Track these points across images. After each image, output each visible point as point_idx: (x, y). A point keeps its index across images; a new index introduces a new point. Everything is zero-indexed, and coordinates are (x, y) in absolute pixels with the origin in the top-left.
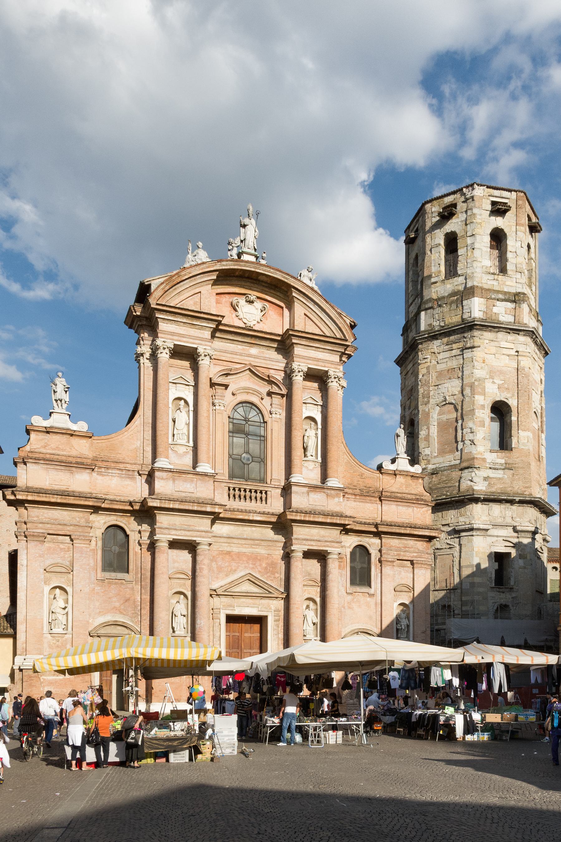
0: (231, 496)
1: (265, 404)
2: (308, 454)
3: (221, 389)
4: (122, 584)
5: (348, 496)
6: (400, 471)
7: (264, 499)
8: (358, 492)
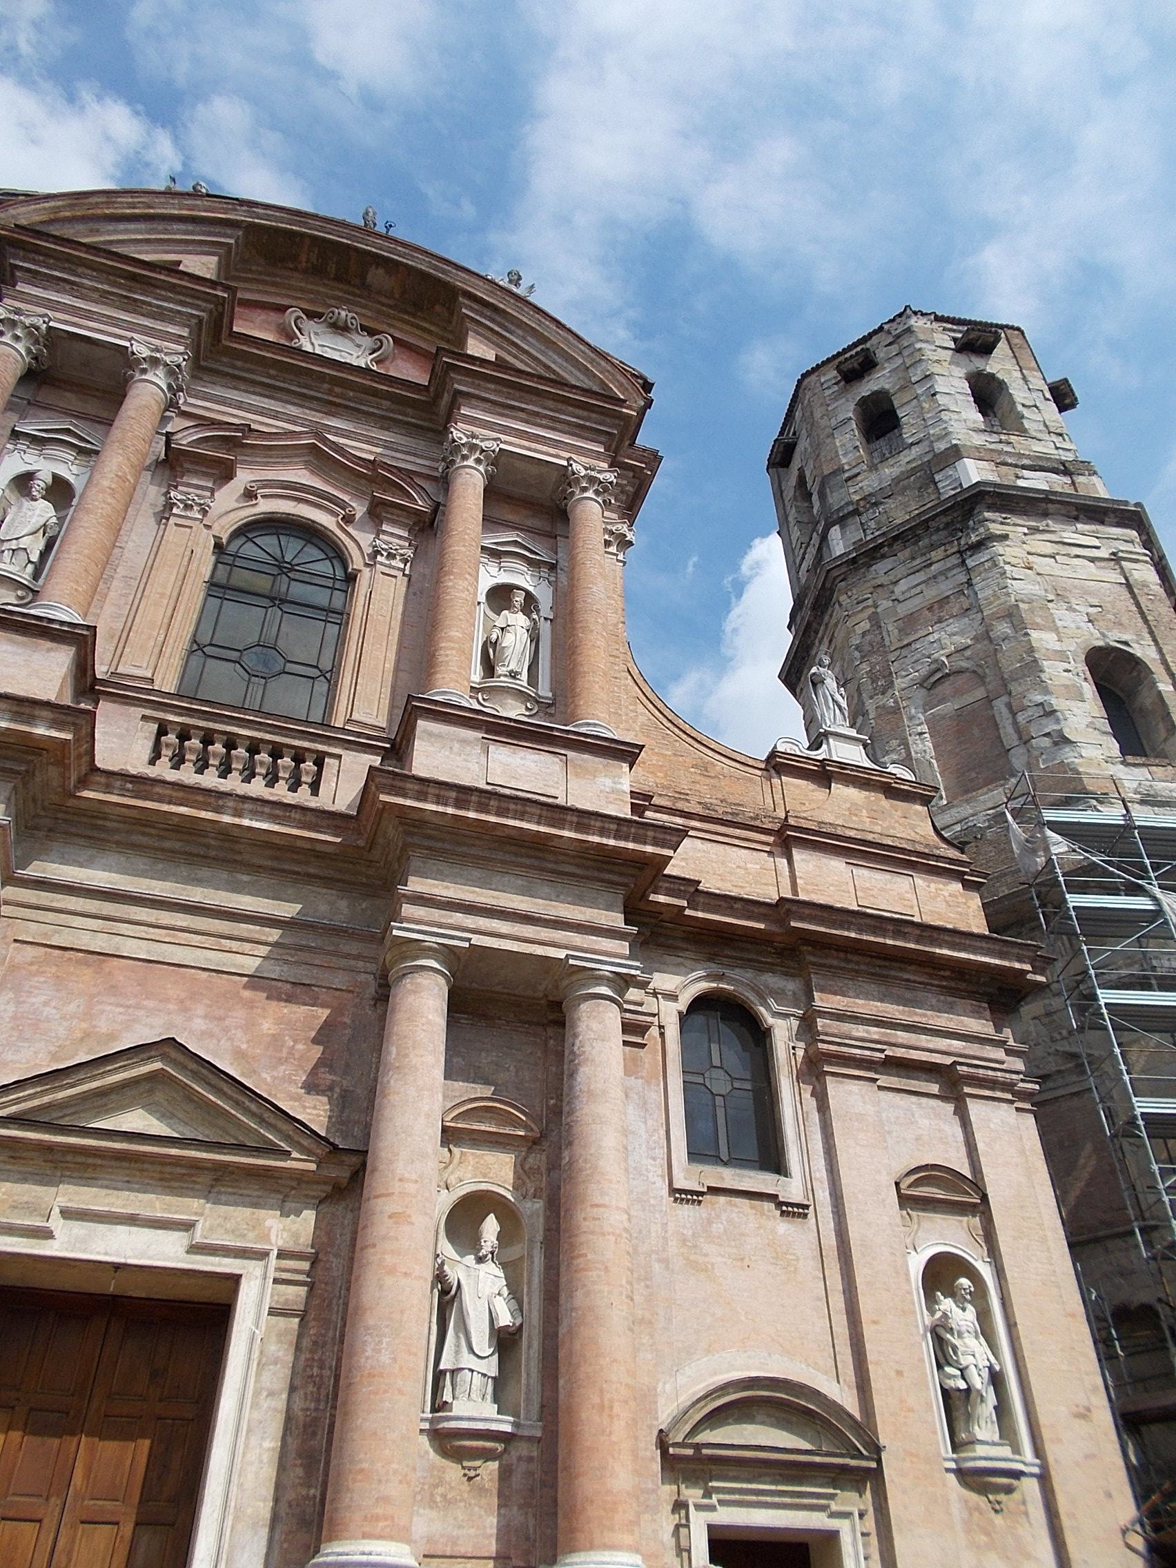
0: (167, 752)
1: (358, 542)
2: (500, 670)
6: (842, 766)
7: (306, 779)
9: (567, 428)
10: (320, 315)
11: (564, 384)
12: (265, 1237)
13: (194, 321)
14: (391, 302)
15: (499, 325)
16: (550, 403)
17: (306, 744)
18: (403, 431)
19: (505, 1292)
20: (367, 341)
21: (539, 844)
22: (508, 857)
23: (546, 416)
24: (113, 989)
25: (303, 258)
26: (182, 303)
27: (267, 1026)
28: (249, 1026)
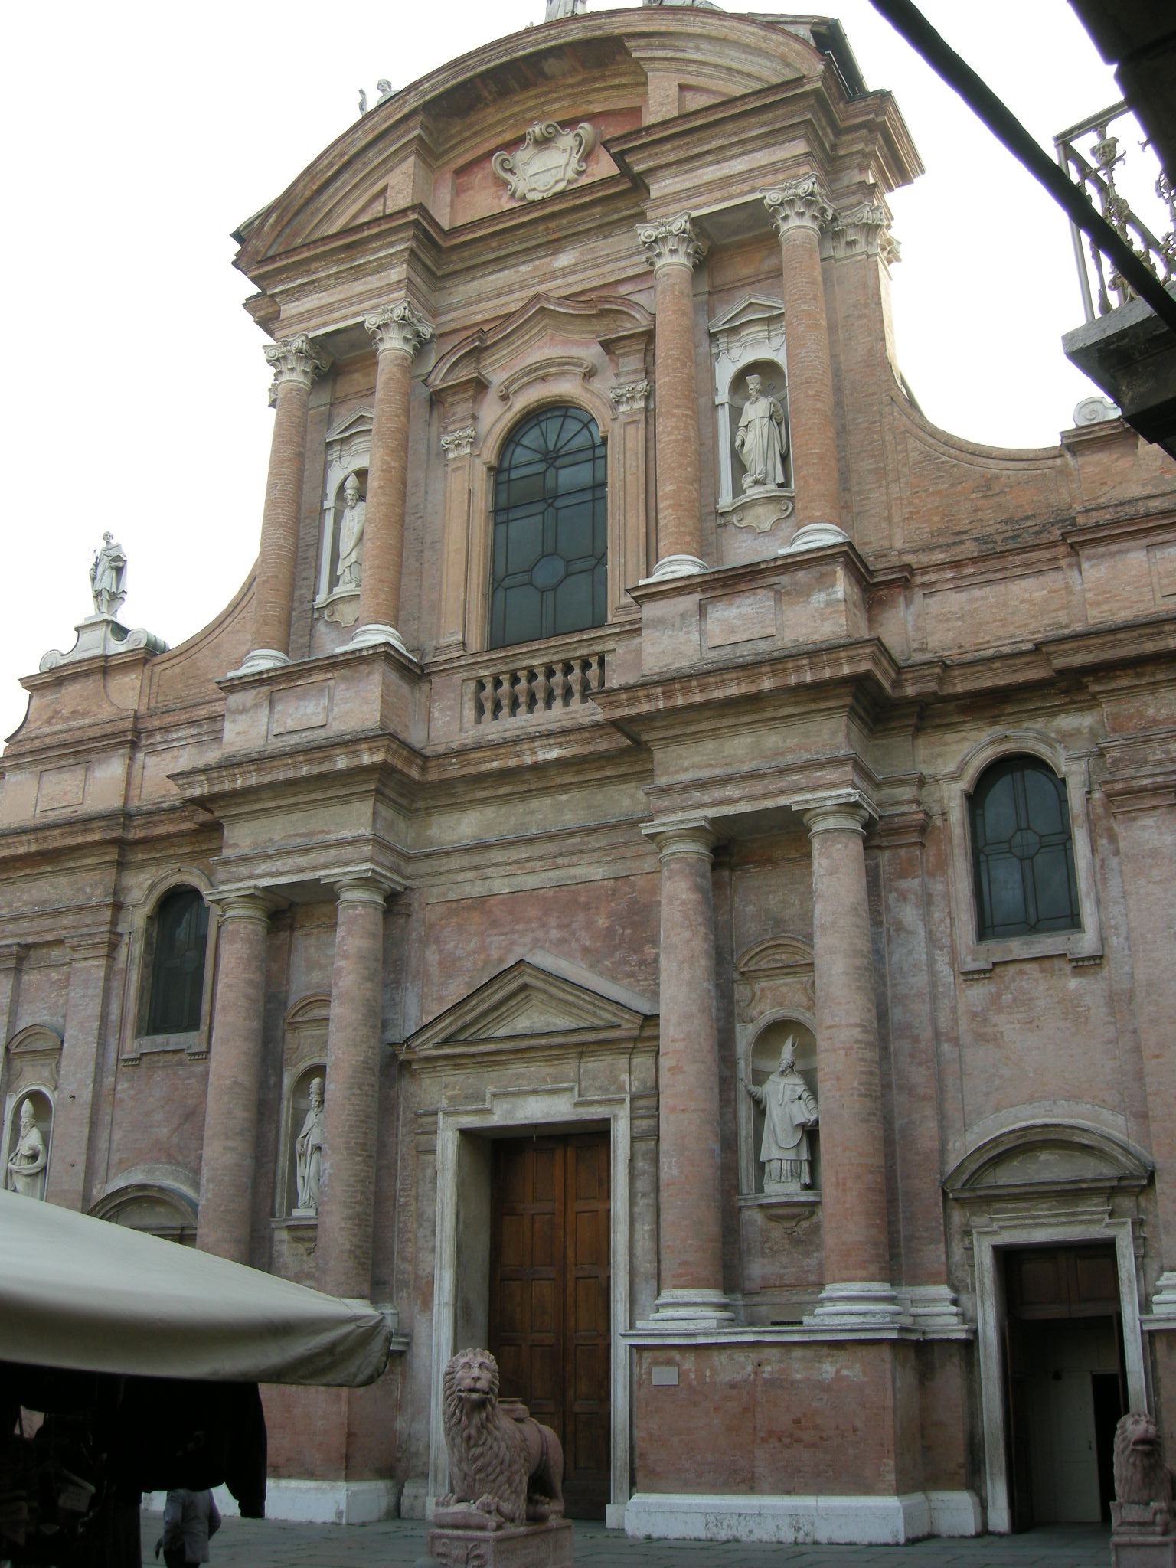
2: (747, 481)
3: (465, 400)
4: (181, 1063)
5: (926, 578)
8: (970, 549)
9: (759, 143)
10: (520, 140)
11: (733, 101)
12: (621, 1089)
13: (407, 254)
14: (579, 78)
15: (672, 48)
16: (730, 127)
17: (584, 651)
18: (624, 229)
19: (805, 1095)
20: (567, 140)
21: (753, 701)
22: (731, 721)
23: (733, 144)
24: (494, 924)
25: (486, 93)
26: (391, 244)
27: (602, 922)
28: (590, 924)
